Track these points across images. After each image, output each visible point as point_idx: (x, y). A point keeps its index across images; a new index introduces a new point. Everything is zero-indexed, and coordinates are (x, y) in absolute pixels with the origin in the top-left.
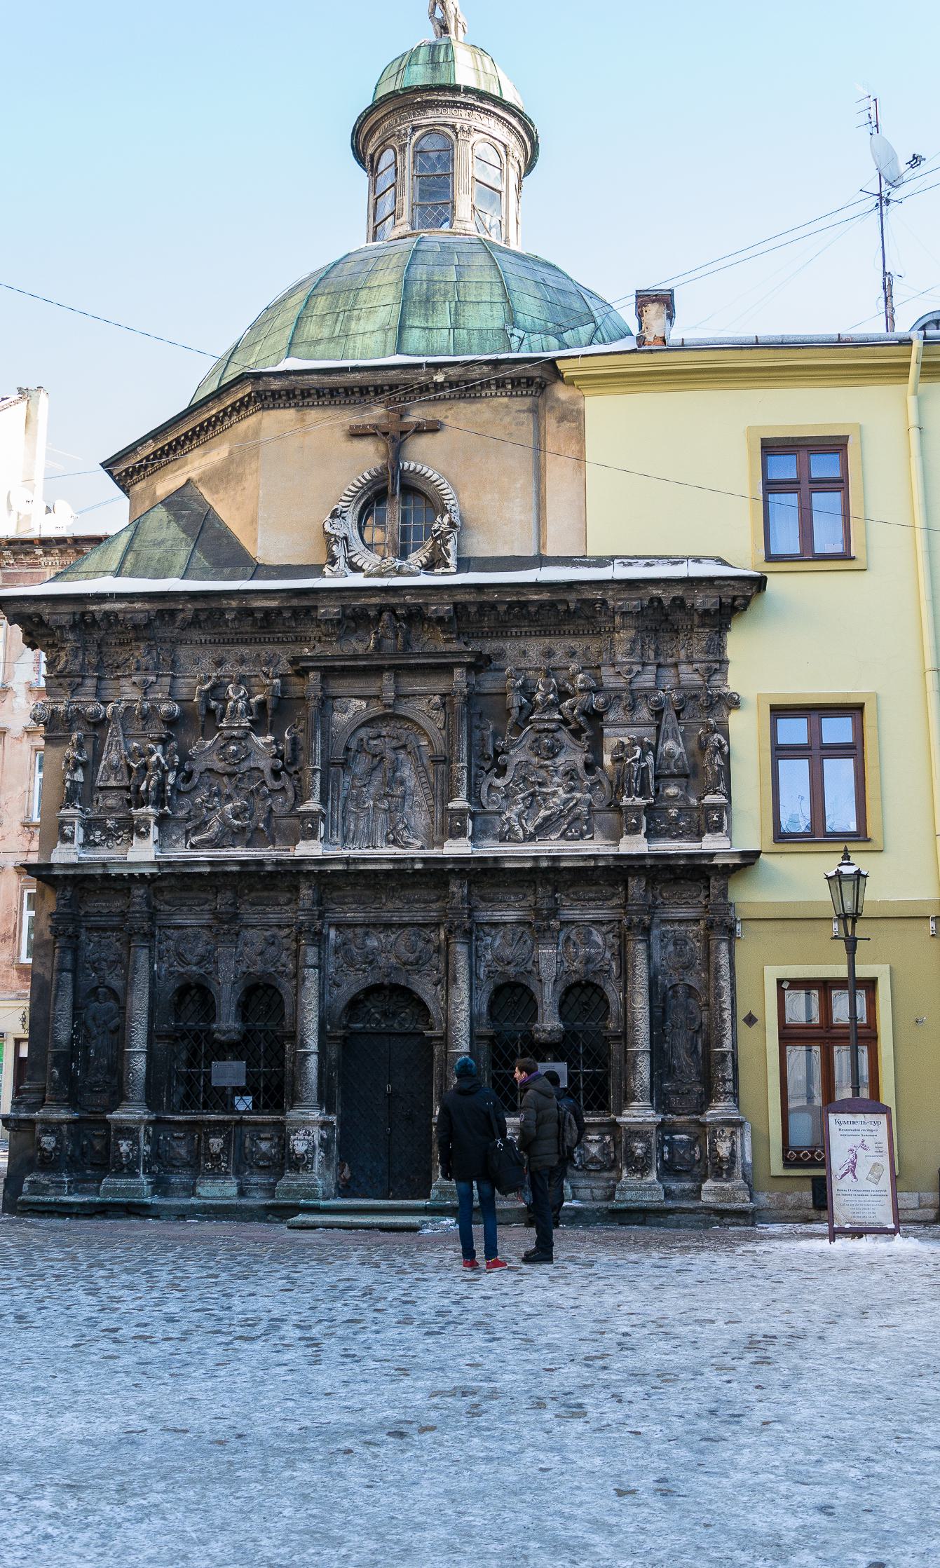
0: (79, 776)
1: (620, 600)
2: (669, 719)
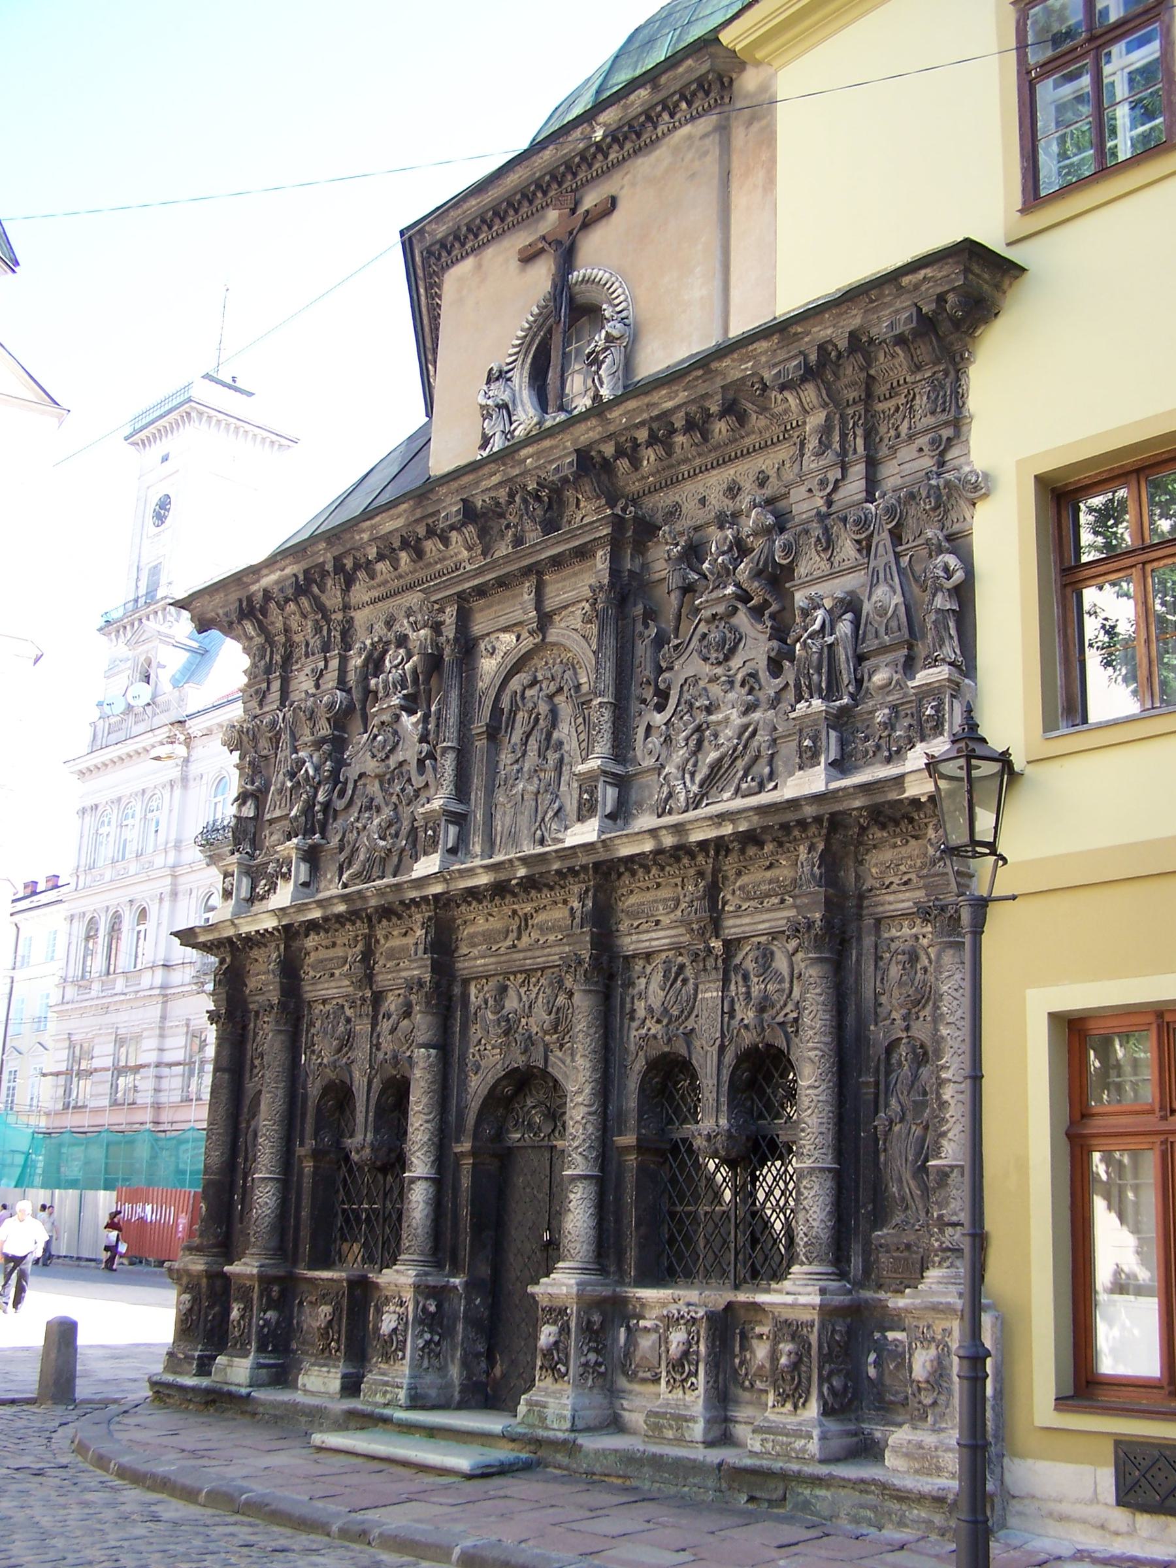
0: (249, 811)
1: (775, 365)
2: (881, 550)
